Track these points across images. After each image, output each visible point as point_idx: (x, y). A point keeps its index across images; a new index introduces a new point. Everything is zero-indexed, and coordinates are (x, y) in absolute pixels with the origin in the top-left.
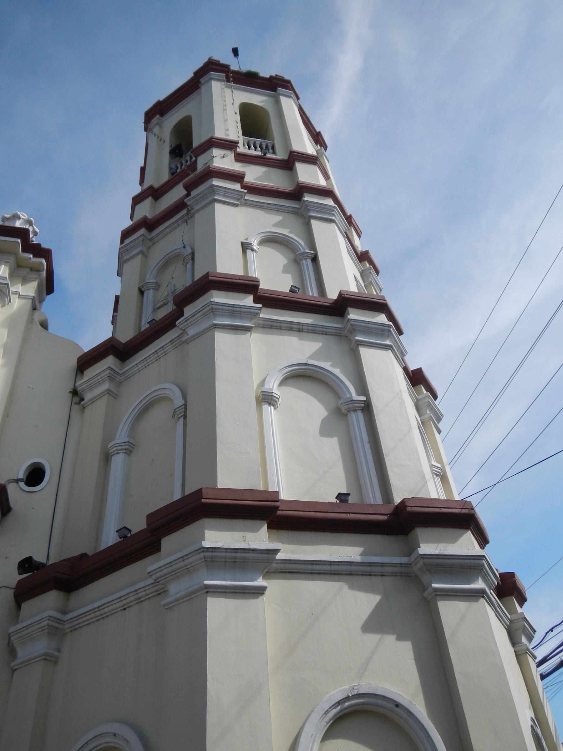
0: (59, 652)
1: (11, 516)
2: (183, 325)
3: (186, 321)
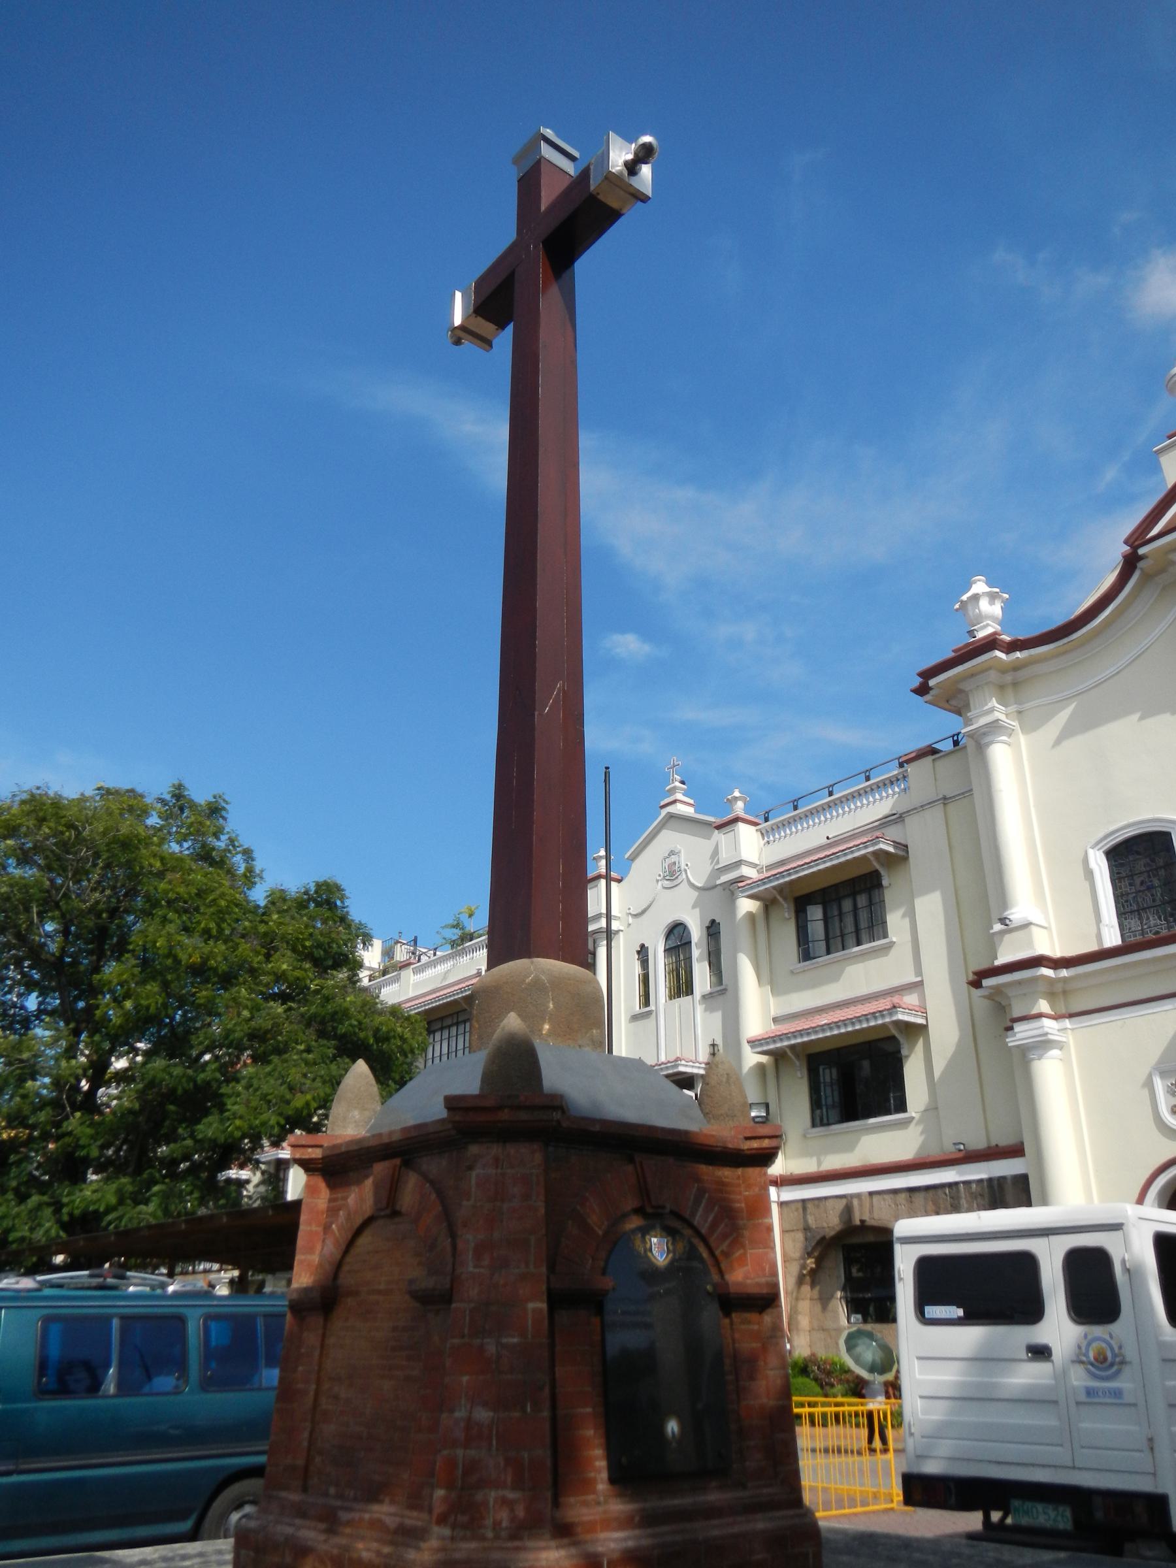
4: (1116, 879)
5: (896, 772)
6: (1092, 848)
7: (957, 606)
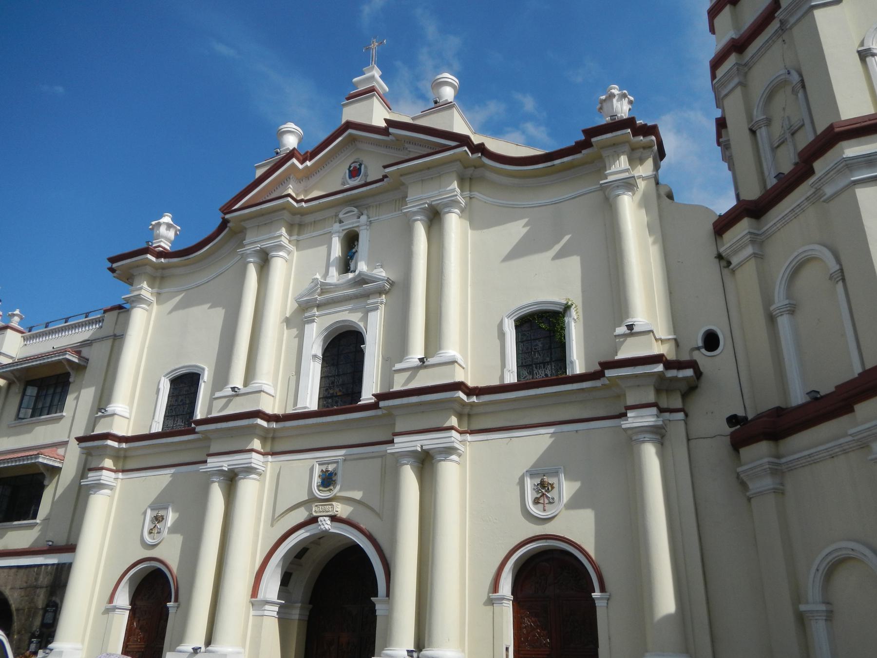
0: (783, 486)
1: (703, 379)
2: (818, 184)
3: (820, 180)
4: (171, 396)
5: (99, 316)
6: (165, 376)
7: (151, 227)
